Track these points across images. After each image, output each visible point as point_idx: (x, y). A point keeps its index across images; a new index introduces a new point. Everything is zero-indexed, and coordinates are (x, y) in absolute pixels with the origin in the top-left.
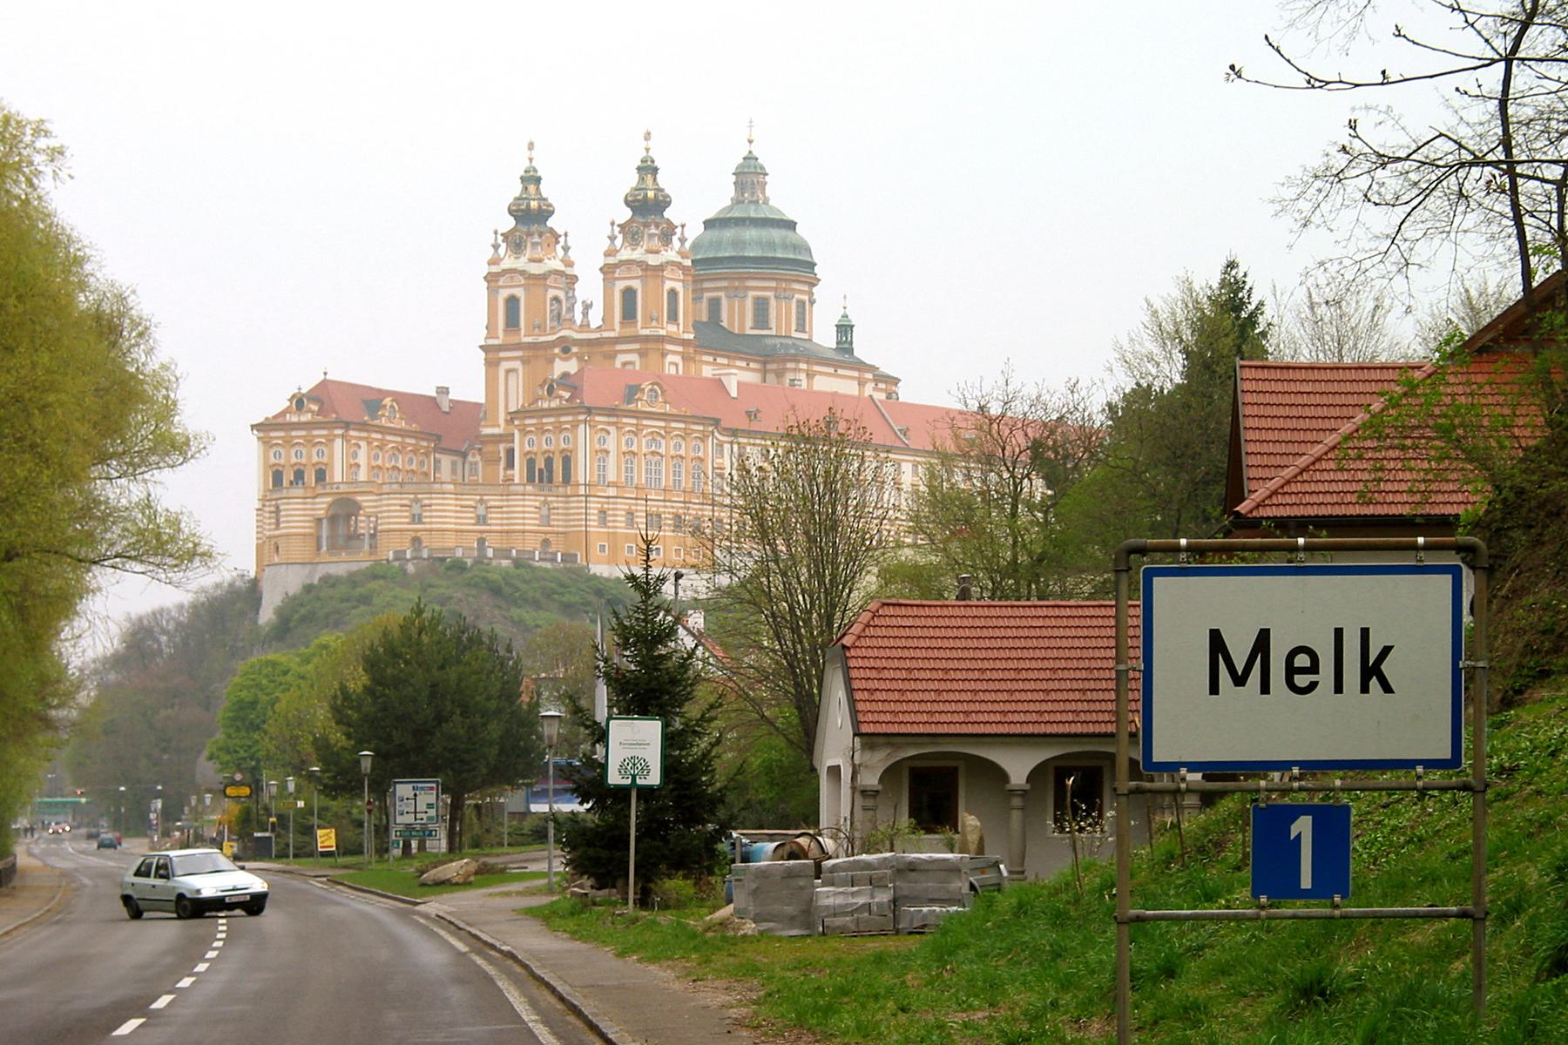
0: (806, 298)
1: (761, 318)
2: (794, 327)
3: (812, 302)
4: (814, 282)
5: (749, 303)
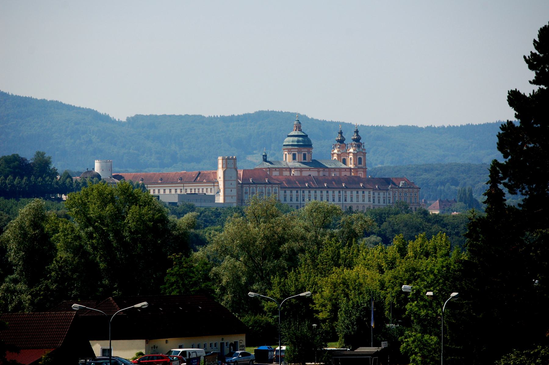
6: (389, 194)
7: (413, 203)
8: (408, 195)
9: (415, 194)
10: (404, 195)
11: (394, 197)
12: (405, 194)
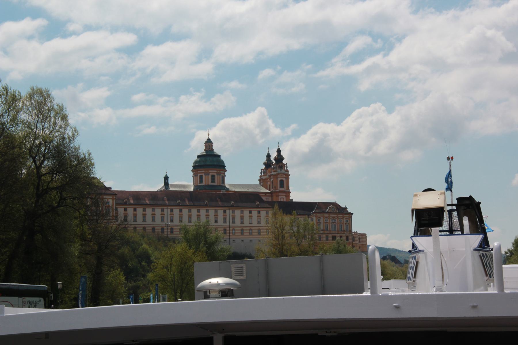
0: (223, 175)
1: (213, 180)
2: (221, 182)
3: (225, 176)
4: (226, 171)
5: (210, 177)
6: (312, 220)
7: (344, 231)
8: (336, 222)
9: (347, 221)
10: (331, 222)
11: (319, 223)
12: (332, 220)
